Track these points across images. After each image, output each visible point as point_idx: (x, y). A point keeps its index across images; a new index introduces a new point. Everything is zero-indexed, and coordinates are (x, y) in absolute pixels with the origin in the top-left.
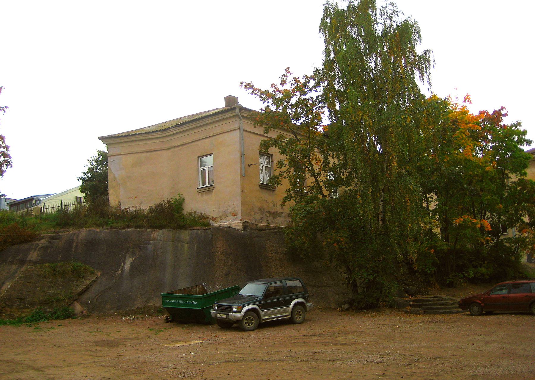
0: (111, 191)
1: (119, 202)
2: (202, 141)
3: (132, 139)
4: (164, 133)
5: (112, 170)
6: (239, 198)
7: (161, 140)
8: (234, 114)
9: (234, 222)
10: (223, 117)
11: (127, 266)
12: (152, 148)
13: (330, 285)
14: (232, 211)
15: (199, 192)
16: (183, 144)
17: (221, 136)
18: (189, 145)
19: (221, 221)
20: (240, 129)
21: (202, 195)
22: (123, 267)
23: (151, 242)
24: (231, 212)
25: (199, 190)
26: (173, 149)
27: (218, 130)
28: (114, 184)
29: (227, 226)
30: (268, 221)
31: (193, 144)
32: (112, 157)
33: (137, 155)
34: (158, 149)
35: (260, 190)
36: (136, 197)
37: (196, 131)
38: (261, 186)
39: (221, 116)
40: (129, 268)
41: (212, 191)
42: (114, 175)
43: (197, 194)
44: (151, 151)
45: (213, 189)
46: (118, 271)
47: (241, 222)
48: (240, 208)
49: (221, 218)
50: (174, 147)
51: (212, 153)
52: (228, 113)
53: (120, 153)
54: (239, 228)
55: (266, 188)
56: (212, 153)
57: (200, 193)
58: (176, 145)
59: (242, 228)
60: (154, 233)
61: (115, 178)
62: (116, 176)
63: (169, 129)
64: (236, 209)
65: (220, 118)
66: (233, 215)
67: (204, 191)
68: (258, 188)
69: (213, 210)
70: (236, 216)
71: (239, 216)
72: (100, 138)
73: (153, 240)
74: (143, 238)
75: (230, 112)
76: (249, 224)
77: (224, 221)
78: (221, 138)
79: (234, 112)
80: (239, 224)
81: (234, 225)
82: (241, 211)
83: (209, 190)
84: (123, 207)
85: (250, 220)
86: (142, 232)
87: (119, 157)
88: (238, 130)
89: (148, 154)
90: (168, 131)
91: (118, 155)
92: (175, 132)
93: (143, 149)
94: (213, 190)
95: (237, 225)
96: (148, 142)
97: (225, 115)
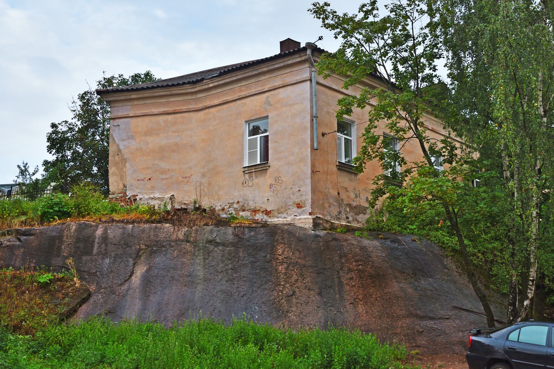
2: (252, 98)
3: (146, 95)
4: (194, 86)
6: (309, 181)
8: (303, 58)
9: (300, 217)
10: (285, 63)
12: (178, 108)
13: (447, 317)
14: (297, 201)
15: (246, 172)
19: (280, 215)
20: (311, 80)
21: (250, 177)
24: (294, 203)
25: (246, 169)
26: (207, 110)
27: (278, 82)
28: (117, 158)
29: (288, 222)
30: (347, 218)
32: (117, 120)
33: (153, 119)
34: (185, 110)
35: (338, 172)
36: (150, 179)
37: (243, 83)
38: (339, 166)
39: (282, 61)
41: (266, 172)
42: (118, 146)
43: (243, 176)
44: (174, 113)
45: (268, 168)
47: (310, 217)
48: (309, 196)
51: (268, 116)
53: (129, 114)
54: (307, 226)
55: (346, 169)
56: (268, 116)
59: (311, 226)
61: (120, 150)
62: (121, 147)
63: (203, 81)
64: (304, 198)
65: (282, 65)
66: (298, 207)
67: (253, 170)
68: (335, 169)
69: (266, 199)
70: (303, 209)
71: (308, 209)
76: (321, 222)
77: (285, 215)
79: (302, 55)
80: (307, 221)
82: (310, 201)
85: (323, 214)
87: (126, 120)
88: (308, 82)
89: (170, 117)
92: (211, 85)
93: (161, 110)
94: (268, 170)
96: (172, 99)
97: (288, 59)
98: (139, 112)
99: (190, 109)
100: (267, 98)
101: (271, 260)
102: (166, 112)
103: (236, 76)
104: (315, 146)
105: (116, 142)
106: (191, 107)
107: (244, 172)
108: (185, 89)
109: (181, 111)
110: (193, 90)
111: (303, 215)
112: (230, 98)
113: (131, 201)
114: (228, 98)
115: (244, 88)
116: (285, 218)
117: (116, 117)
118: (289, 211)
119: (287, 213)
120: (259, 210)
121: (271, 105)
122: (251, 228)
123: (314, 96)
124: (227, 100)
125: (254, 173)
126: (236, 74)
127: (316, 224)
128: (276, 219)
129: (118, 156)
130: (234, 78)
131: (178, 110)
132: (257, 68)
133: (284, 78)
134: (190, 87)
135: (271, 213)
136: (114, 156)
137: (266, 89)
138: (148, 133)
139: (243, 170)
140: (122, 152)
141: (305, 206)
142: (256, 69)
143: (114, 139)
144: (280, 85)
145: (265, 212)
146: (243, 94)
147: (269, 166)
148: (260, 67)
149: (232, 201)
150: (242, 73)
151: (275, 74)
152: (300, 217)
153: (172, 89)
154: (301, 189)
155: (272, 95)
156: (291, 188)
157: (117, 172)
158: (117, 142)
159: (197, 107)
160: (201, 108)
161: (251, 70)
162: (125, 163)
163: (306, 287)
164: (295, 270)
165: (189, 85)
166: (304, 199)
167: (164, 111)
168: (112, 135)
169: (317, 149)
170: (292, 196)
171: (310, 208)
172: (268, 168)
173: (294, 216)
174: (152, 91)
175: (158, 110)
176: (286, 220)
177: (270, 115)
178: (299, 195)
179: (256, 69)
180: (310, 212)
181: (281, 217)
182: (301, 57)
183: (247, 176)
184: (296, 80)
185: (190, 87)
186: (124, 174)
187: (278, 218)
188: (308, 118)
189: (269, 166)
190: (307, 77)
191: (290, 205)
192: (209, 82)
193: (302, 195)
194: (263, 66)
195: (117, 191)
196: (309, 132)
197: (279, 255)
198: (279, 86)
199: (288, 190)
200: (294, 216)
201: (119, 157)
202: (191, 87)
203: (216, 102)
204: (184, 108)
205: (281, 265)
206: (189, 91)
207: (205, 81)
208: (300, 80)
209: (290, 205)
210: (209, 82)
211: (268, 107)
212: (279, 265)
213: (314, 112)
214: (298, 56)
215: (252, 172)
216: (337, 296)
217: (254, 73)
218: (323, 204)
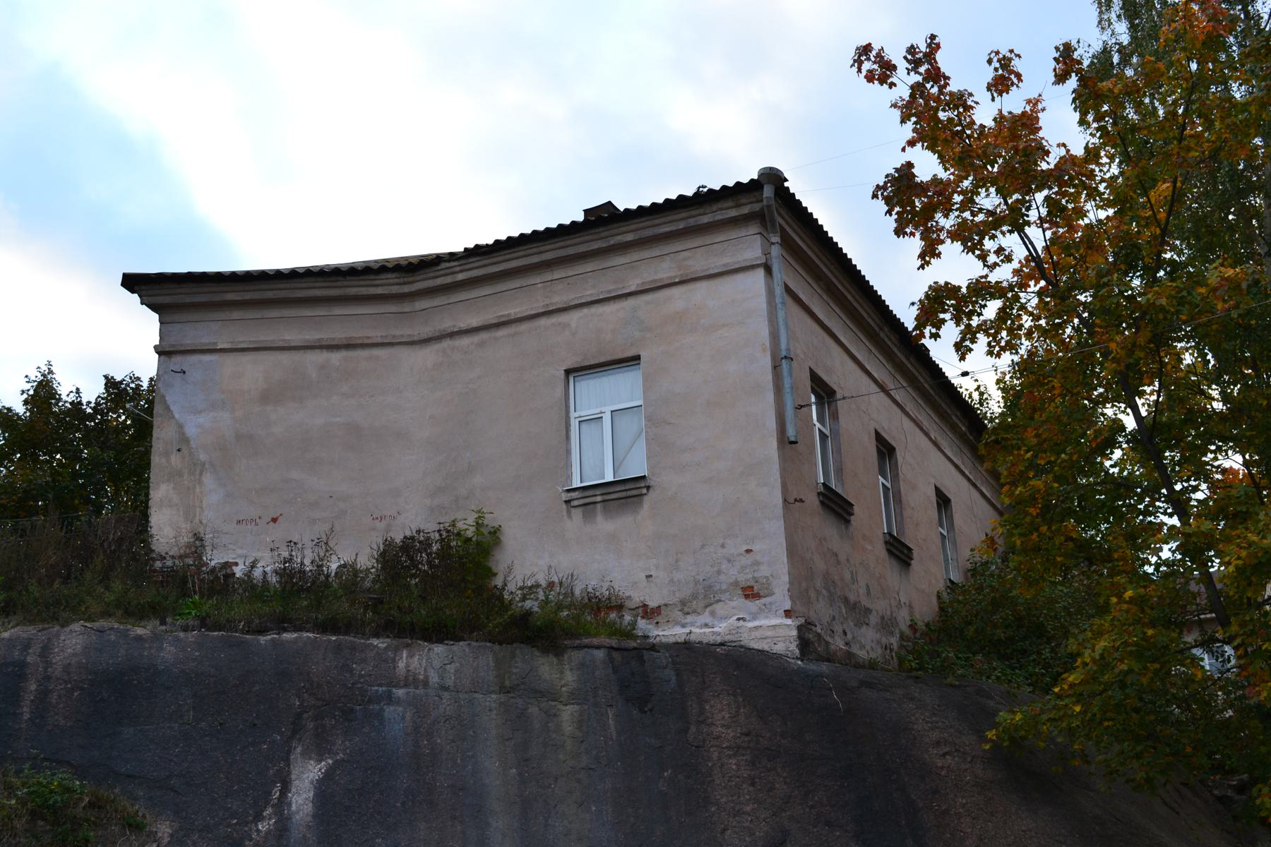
0: (161, 493)
2: (585, 311)
3: (269, 295)
4: (411, 279)
5: (172, 408)
6: (776, 527)
8: (745, 210)
9: (756, 623)
10: (692, 222)
11: (301, 798)
14: (745, 578)
15: (575, 503)
16: (494, 322)
17: (675, 291)
18: (524, 327)
19: (689, 619)
22: (283, 800)
23: (400, 692)
24: (736, 584)
26: (446, 343)
28: (175, 459)
29: (719, 639)
31: (543, 321)
33: (285, 358)
34: (379, 340)
36: (274, 520)
37: (558, 274)
39: (684, 215)
40: (309, 808)
41: (641, 503)
43: (565, 513)
44: (349, 346)
45: (644, 491)
46: (259, 817)
47: (789, 622)
49: (685, 607)
50: (452, 335)
51: (637, 358)
52: (715, 208)
53: (215, 343)
54: (779, 648)
55: (834, 506)
56: (637, 358)
57: (579, 510)
58: (463, 325)
59: (794, 647)
60: (411, 656)
61: (184, 439)
62: (191, 431)
64: (764, 571)
65: (681, 225)
66: (747, 597)
67: (599, 499)
69: (643, 575)
70: (763, 600)
72: (132, 282)
73: (406, 686)
74: (361, 676)
77: (705, 618)
78: (677, 298)
79: (743, 201)
80: (782, 632)
81: (758, 634)
82: (786, 578)
83: (624, 494)
84: (215, 558)
86: (353, 648)
88: (760, 273)
89: (336, 357)
92: (460, 277)
94: (646, 498)
95: (769, 633)
97: (701, 211)
101: (704, 741)
102: (324, 343)
103: (541, 253)
104: (791, 433)
105: (173, 417)
107: (567, 502)
108: (382, 285)
109: (369, 341)
110: (406, 289)
111: (767, 617)
112: (518, 310)
116: (706, 625)
118: (718, 607)
119: (713, 614)
122: (626, 650)
123: (779, 306)
124: (509, 315)
125: (599, 506)
126: (542, 249)
127: (805, 644)
130: (535, 259)
131: (360, 338)
132: (607, 233)
133: (685, 259)
134: (398, 281)
135: (659, 614)
136: (167, 454)
137: (633, 288)
139: (565, 497)
141: (771, 594)
143: (168, 408)
145: (640, 610)
146: (559, 300)
147: (648, 488)
148: (614, 231)
150: (558, 245)
151: (656, 251)
152: (756, 623)
153: (345, 283)
154: (756, 547)
156: (723, 546)
158: (177, 416)
161: (587, 238)
162: (201, 474)
164: (779, 770)
165: (394, 275)
166: (767, 573)
167: (319, 340)
168: (163, 397)
169: (795, 443)
171: (787, 598)
172: (644, 491)
173: (739, 619)
174: (287, 286)
177: (643, 355)
178: (749, 562)
180: (788, 607)
181: (692, 624)
182: (738, 206)
183: (577, 514)
185: (398, 281)
187: (683, 626)
188: (767, 362)
189: (648, 488)
192: (458, 269)
193: (757, 563)
194: (624, 229)
195: (175, 551)
196: (770, 397)
197: (723, 726)
198: (669, 281)
200: (739, 619)
202: (401, 280)
203: (474, 322)
204: (376, 334)
205: (735, 755)
206: (395, 290)
207: (443, 265)
208: (737, 266)
210: (458, 269)
212: (730, 757)
213: (783, 346)
214: (730, 203)
215: (595, 503)
217: (596, 247)
218: (807, 590)
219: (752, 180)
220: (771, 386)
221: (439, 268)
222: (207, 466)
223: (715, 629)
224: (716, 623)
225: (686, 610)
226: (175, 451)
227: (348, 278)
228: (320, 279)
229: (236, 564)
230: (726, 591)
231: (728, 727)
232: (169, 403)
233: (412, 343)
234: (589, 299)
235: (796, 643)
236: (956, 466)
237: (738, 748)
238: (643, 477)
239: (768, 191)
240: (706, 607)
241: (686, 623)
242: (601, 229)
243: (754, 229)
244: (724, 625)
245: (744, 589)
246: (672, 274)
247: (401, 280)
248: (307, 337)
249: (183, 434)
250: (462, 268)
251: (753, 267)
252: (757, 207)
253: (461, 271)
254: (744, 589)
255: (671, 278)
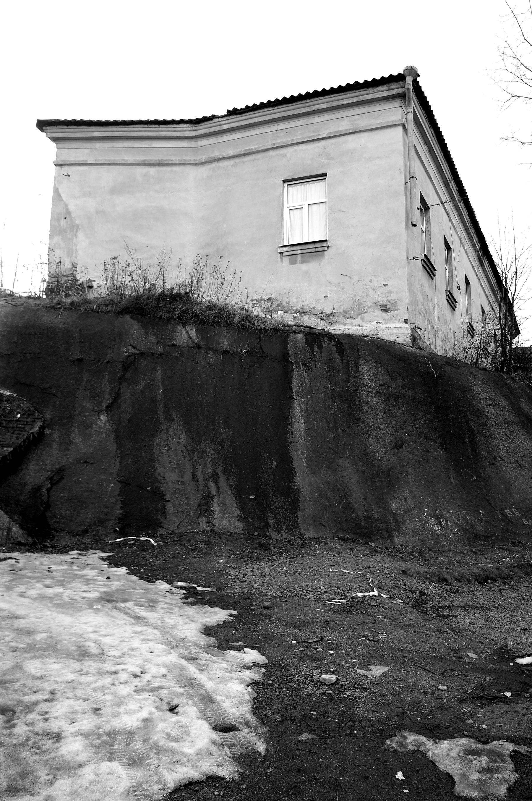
1: (74, 265)
2: (296, 147)
3: (117, 134)
5: (62, 195)
7: (184, 144)
8: (394, 92)
9: (388, 325)
10: (361, 98)
12: (165, 158)
14: (382, 300)
15: (285, 254)
16: (243, 153)
17: (350, 138)
18: (259, 156)
19: (348, 321)
24: (376, 303)
26: (214, 165)
27: (344, 125)
29: (365, 333)
31: (271, 153)
34: (177, 162)
41: (323, 256)
42: (66, 205)
44: (160, 164)
45: (326, 248)
47: (407, 326)
49: (347, 315)
50: (218, 160)
51: (325, 175)
53: (86, 161)
54: (400, 340)
56: (325, 175)
58: (225, 155)
59: (408, 340)
62: (72, 208)
65: (355, 100)
66: (383, 310)
67: (299, 252)
75: (384, 88)
77: (358, 321)
80: (401, 331)
81: (388, 331)
88: (400, 128)
89: (152, 171)
90: (207, 124)
91: (79, 165)
92: (225, 127)
93: (140, 158)
94: (326, 252)
95: (395, 332)
97: (367, 92)
98: (102, 158)
99: (185, 160)
100: (325, 147)
101: (358, 387)
102: (146, 162)
105: (62, 200)
106: (187, 158)
107: (280, 253)
109: (172, 162)
110: (193, 134)
111: (394, 322)
112: (257, 146)
113: (83, 288)
114: (254, 147)
115: (281, 134)
116: (358, 325)
117: (66, 163)
118: (366, 315)
119: (362, 319)
120: (310, 312)
121: (332, 158)
124: (252, 149)
125: (299, 255)
126: (272, 112)
127: (414, 340)
128: (342, 327)
129: (65, 220)
131: (166, 160)
132: (311, 103)
133: (356, 120)
134: (189, 129)
137: (324, 136)
138: (115, 191)
140: (73, 215)
141: (397, 310)
142: (309, 104)
144: (350, 130)
146: (281, 141)
147: (328, 247)
149: (259, 297)
152: (388, 325)
153: (160, 129)
155: (332, 144)
156: (370, 281)
157: (62, 244)
158: (64, 199)
159: (198, 159)
160: (203, 161)
161: (300, 106)
162: (76, 231)
163: (421, 434)
164: (400, 406)
165: (188, 125)
167: (144, 161)
170: (371, 293)
172: (326, 248)
173: (377, 323)
175: (134, 158)
176: (362, 330)
178: (385, 291)
179: (309, 104)
181: (350, 324)
183: (286, 260)
184: (379, 124)
185: (189, 129)
186: (74, 248)
187: (345, 325)
190: (399, 120)
191: (369, 307)
192: (224, 122)
199: (364, 283)
200: (377, 323)
201: (67, 222)
202: (191, 129)
203: (231, 153)
206: (187, 134)
207: (215, 120)
209: (369, 307)
210: (224, 122)
211: (326, 161)
212: (372, 397)
216: (470, 451)
217: (304, 111)
219: (400, 74)
220: (403, 193)
221: (213, 122)
222: (80, 227)
223: (364, 328)
224: (364, 324)
225: (347, 316)
226: (63, 219)
227: (161, 126)
228: (145, 126)
229: (94, 281)
230: (371, 307)
231: (372, 380)
232: (60, 192)
233: (196, 164)
234: (299, 141)
235: (410, 338)
236: (473, 267)
237: (377, 392)
238: (326, 241)
239: (409, 80)
240: (359, 315)
241: (347, 324)
242: (308, 101)
243: (397, 103)
244: (368, 325)
245: (382, 306)
246: (348, 128)
247: (191, 129)
248: (137, 159)
249: (68, 209)
250: (226, 122)
251: (396, 125)
252: (400, 91)
253: (226, 124)
254: (382, 306)
255: (347, 130)
